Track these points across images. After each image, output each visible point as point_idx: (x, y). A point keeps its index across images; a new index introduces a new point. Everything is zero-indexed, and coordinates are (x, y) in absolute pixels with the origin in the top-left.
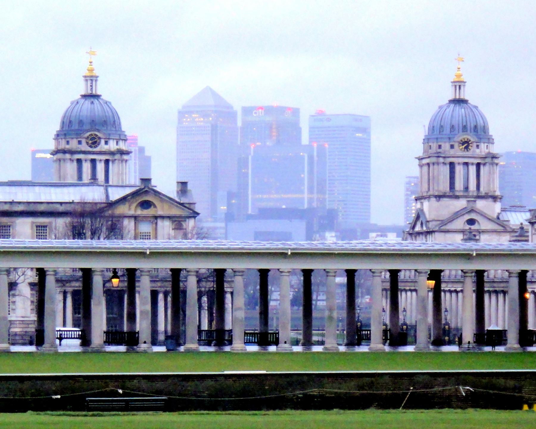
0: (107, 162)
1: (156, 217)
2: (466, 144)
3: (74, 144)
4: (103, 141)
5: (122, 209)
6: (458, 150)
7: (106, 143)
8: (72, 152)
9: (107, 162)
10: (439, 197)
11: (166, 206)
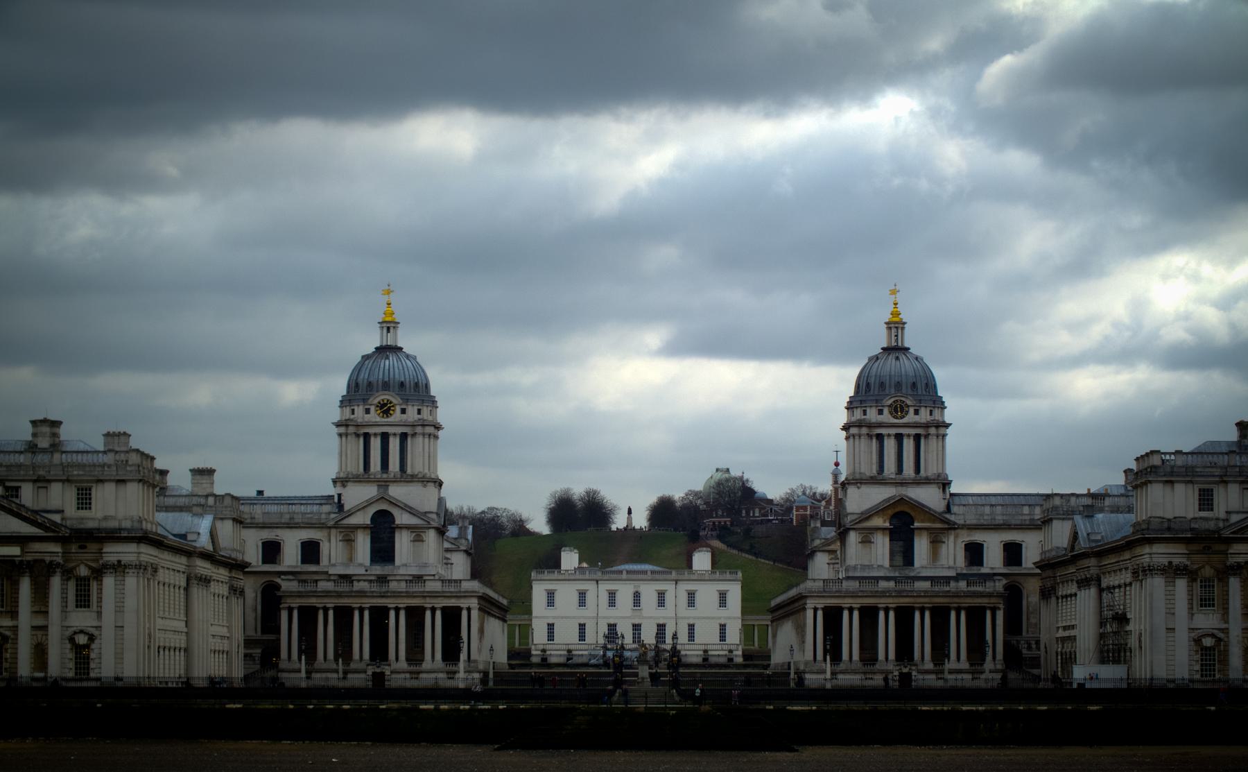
3: (872, 415)
4: (912, 410)
7: (916, 412)
8: (870, 426)
9: (917, 438)
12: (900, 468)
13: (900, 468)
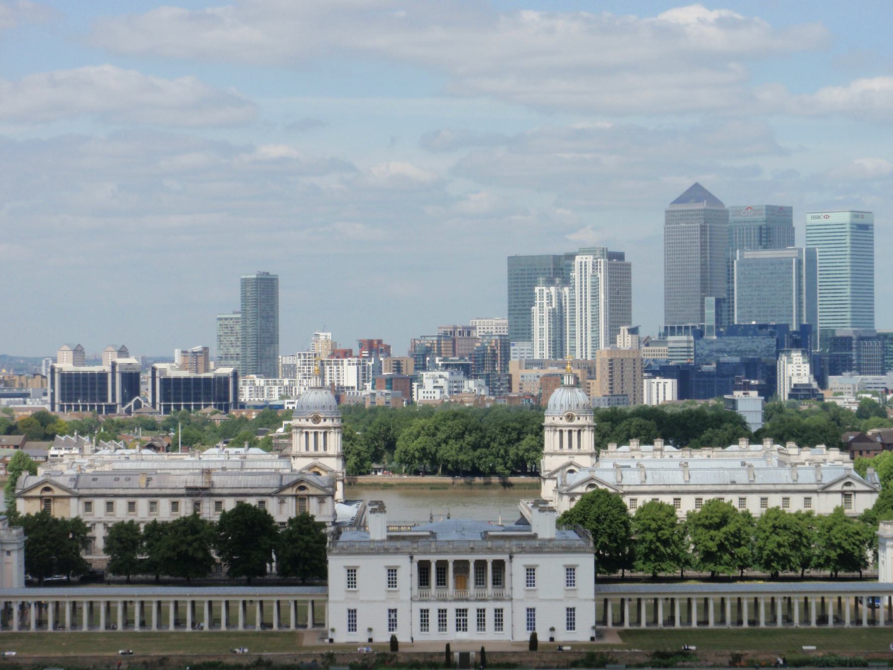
0: (325, 433)
1: (309, 496)
2: (570, 418)
3: (303, 423)
5: (289, 491)
6: (564, 422)
8: (302, 428)
9: (325, 433)
10: (552, 454)
11: (314, 489)
12: (316, 448)
13: (316, 448)
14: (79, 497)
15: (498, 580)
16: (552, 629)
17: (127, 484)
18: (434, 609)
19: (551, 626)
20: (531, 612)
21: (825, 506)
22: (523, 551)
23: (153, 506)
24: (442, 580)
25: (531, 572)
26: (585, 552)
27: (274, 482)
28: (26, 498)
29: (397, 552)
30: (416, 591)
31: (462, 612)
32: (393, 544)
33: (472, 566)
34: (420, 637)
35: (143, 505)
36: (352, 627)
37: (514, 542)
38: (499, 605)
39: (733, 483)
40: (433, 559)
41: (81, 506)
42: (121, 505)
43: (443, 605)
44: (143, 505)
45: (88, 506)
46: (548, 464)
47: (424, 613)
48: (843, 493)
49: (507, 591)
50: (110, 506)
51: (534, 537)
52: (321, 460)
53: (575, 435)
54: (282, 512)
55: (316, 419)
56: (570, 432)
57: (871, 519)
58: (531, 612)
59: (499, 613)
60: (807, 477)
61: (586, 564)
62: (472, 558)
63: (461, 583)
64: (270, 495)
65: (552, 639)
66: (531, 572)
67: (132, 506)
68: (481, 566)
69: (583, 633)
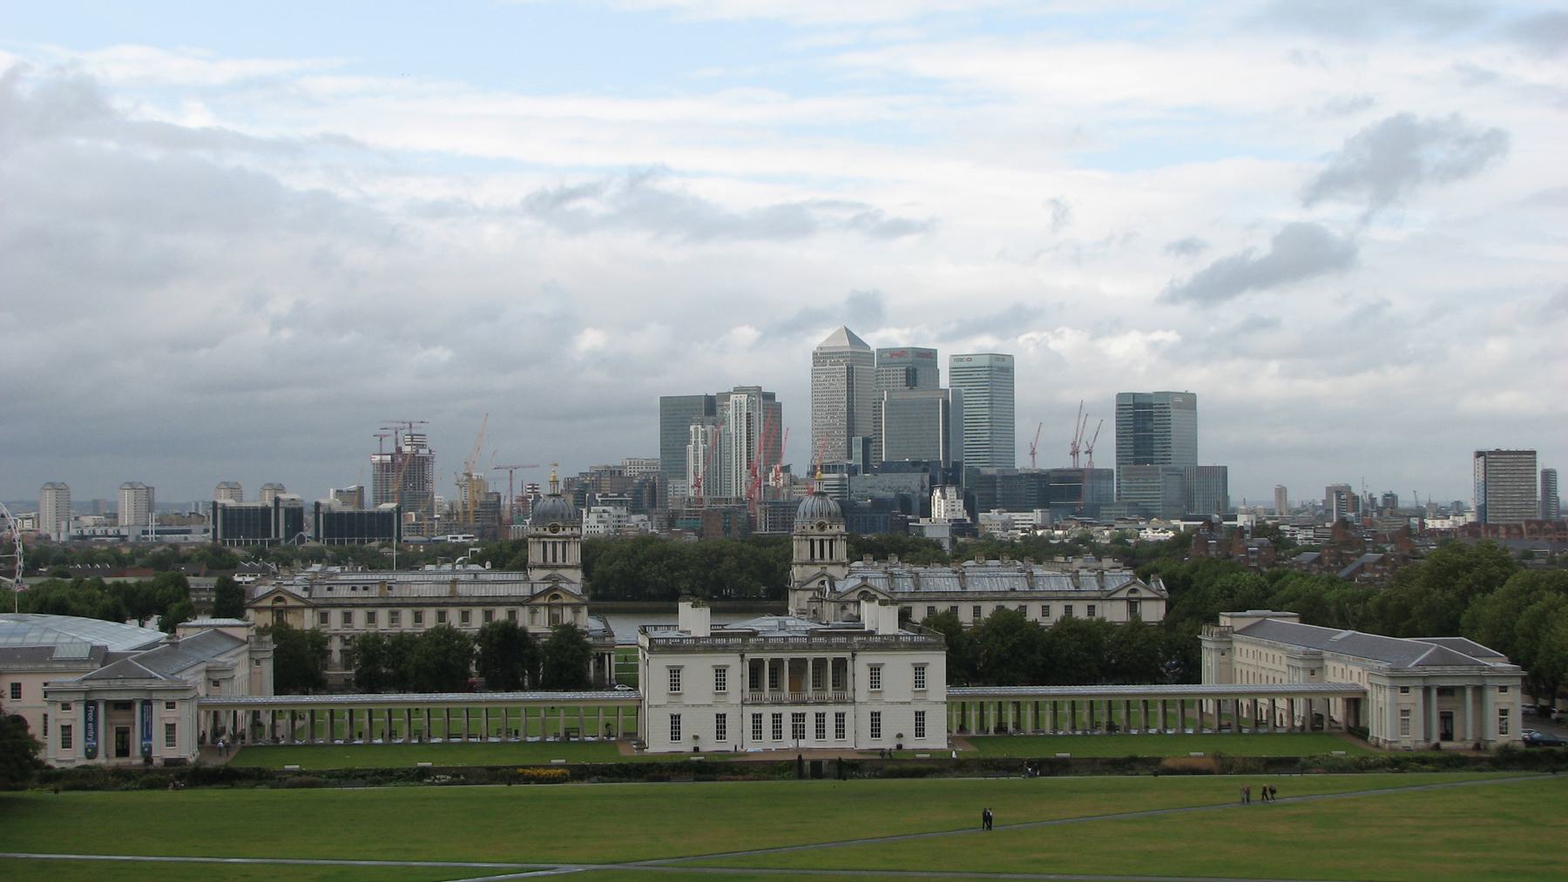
2: (822, 526)
3: (541, 531)
5: (541, 600)
6: (816, 531)
10: (802, 564)
14: (314, 607)
15: (840, 680)
16: (900, 736)
17: (365, 594)
18: (767, 713)
19: (897, 731)
20: (876, 717)
21: (1116, 613)
22: (867, 647)
23: (394, 618)
24: (775, 684)
25: (875, 671)
26: (935, 649)
27: (523, 590)
28: (259, 610)
29: (725, 649)
30: (747, 694)
31: (798, 718)
32: (718, 641)
33: (810, 664)
34: (752, 747)
35: (383, 615)
36: (676, 735)
37: (856, 639)
38: (840, 709)
39: (1013, 590)
40: (767, 657)
41: (316, 619)
42: (359, 616)
43: (777, 709)
44: (383, 615)
45: (324, 618)
46: (797, 573)
47: (757, 718)
48: (1128, 600)
49: (850, 693)
50: (348, 618)
51: (871, 633)
52: (561, 572)
53: (827, 545)
54: (537, 624)
55: (555, 529)
56: (822, 542)
57: (1169, 624)
58: (876, 717)
59: (840, 717)
60: (1091, 584)
61: (937, 663)
62: (810, 656)
63: (796, 686)
64: (521, 604)
65: (900, 747)
66: (875, 671)
67: (371, 618)
68: (820, 664)
69: (936, 739)
